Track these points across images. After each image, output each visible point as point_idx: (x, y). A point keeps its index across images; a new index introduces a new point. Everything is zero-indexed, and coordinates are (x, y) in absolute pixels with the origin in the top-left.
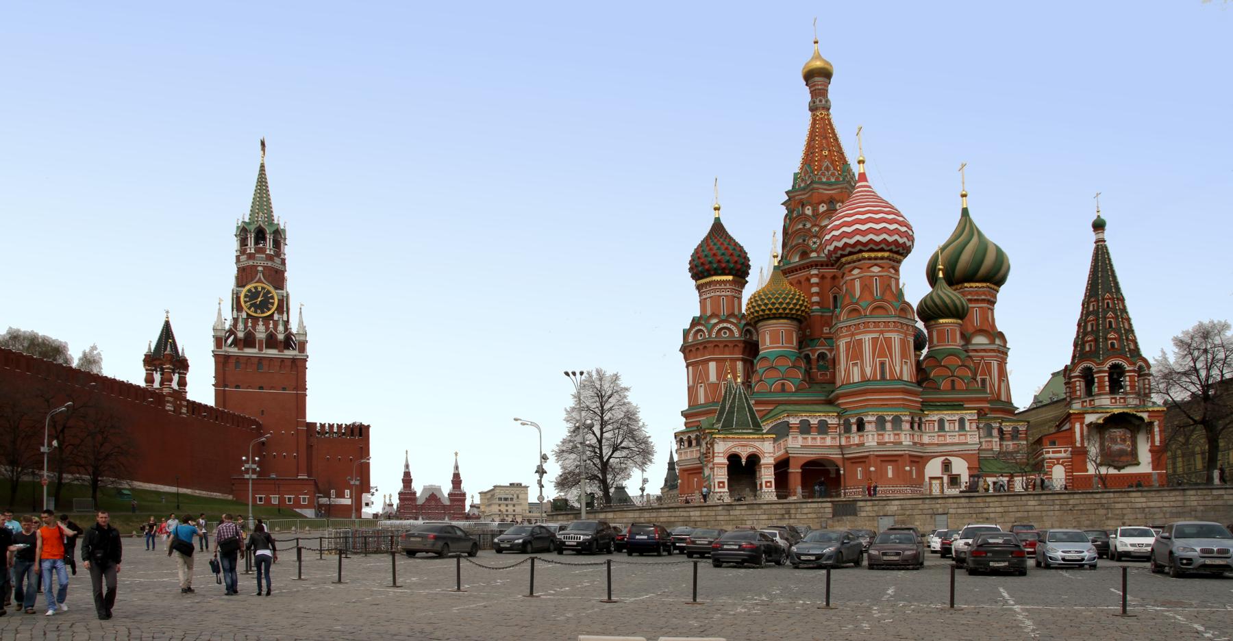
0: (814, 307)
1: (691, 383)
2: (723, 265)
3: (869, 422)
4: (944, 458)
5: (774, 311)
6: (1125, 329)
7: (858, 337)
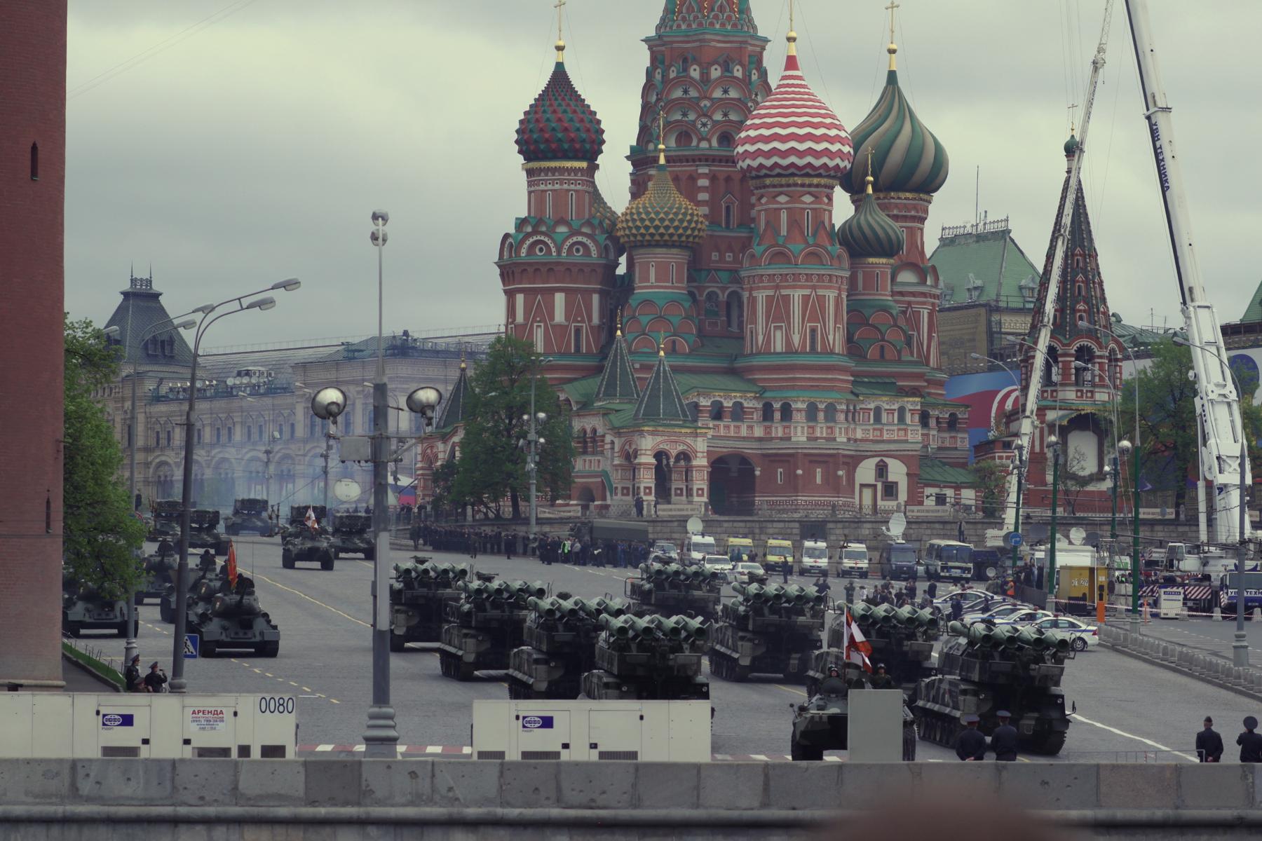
1: (520, 318)
3: (799, 410)
4: (878, 459)
7: (784, 292)
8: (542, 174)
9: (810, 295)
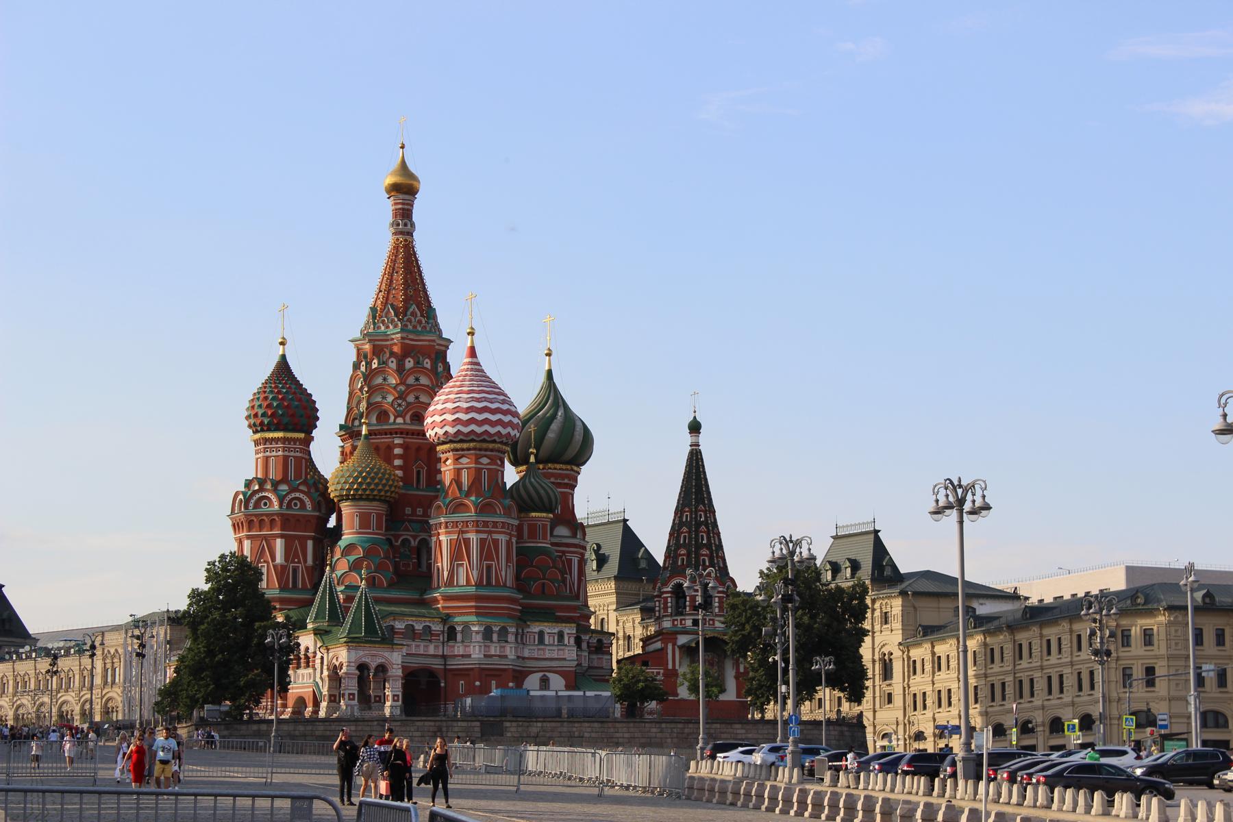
3: (477, 632)
4: (542, 673)
8: (268, 443)
9: (486, 539)
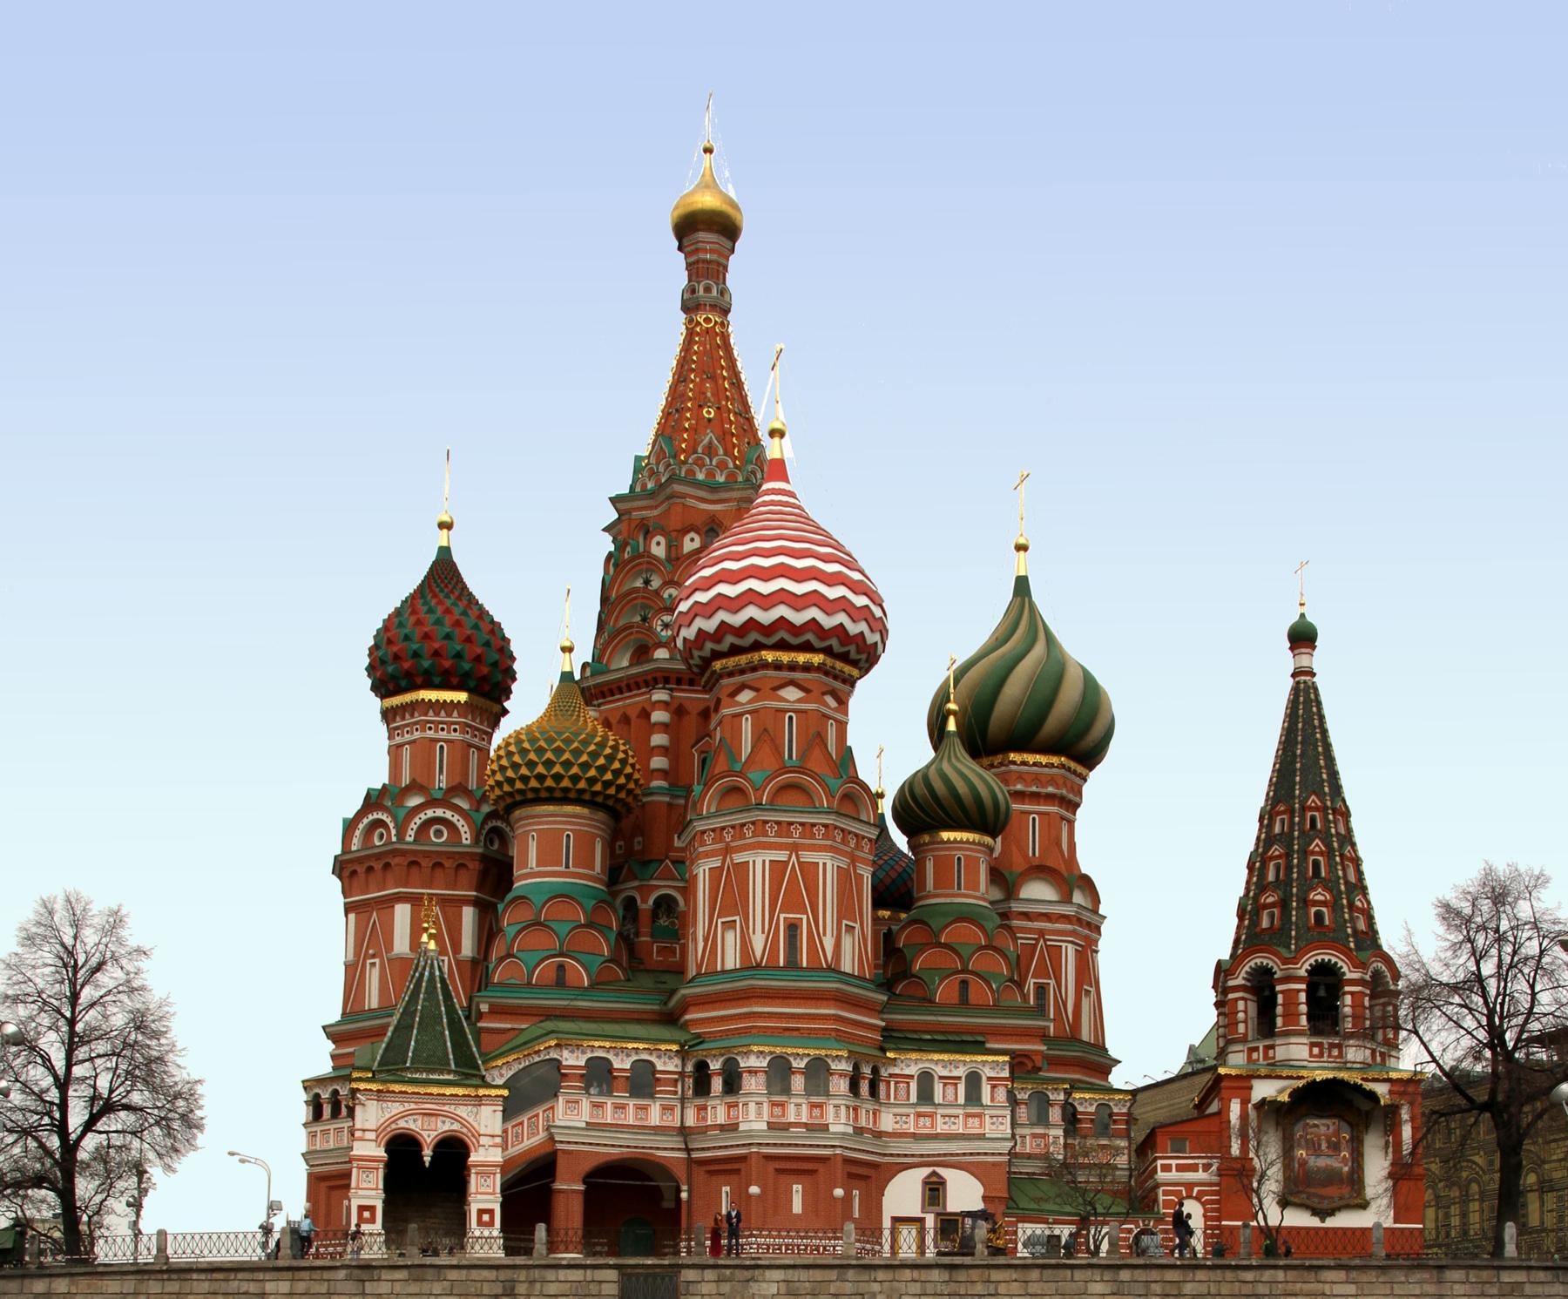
0: (655, 783)
2: (447, 664)
3: (753, 1071)
4: (927, 1171)
5: (549, 783)
6: (1347, 883)
7: (739, 858)
9: (786, 863)
